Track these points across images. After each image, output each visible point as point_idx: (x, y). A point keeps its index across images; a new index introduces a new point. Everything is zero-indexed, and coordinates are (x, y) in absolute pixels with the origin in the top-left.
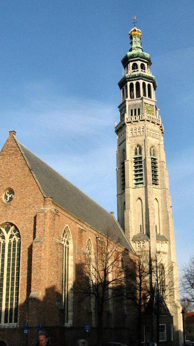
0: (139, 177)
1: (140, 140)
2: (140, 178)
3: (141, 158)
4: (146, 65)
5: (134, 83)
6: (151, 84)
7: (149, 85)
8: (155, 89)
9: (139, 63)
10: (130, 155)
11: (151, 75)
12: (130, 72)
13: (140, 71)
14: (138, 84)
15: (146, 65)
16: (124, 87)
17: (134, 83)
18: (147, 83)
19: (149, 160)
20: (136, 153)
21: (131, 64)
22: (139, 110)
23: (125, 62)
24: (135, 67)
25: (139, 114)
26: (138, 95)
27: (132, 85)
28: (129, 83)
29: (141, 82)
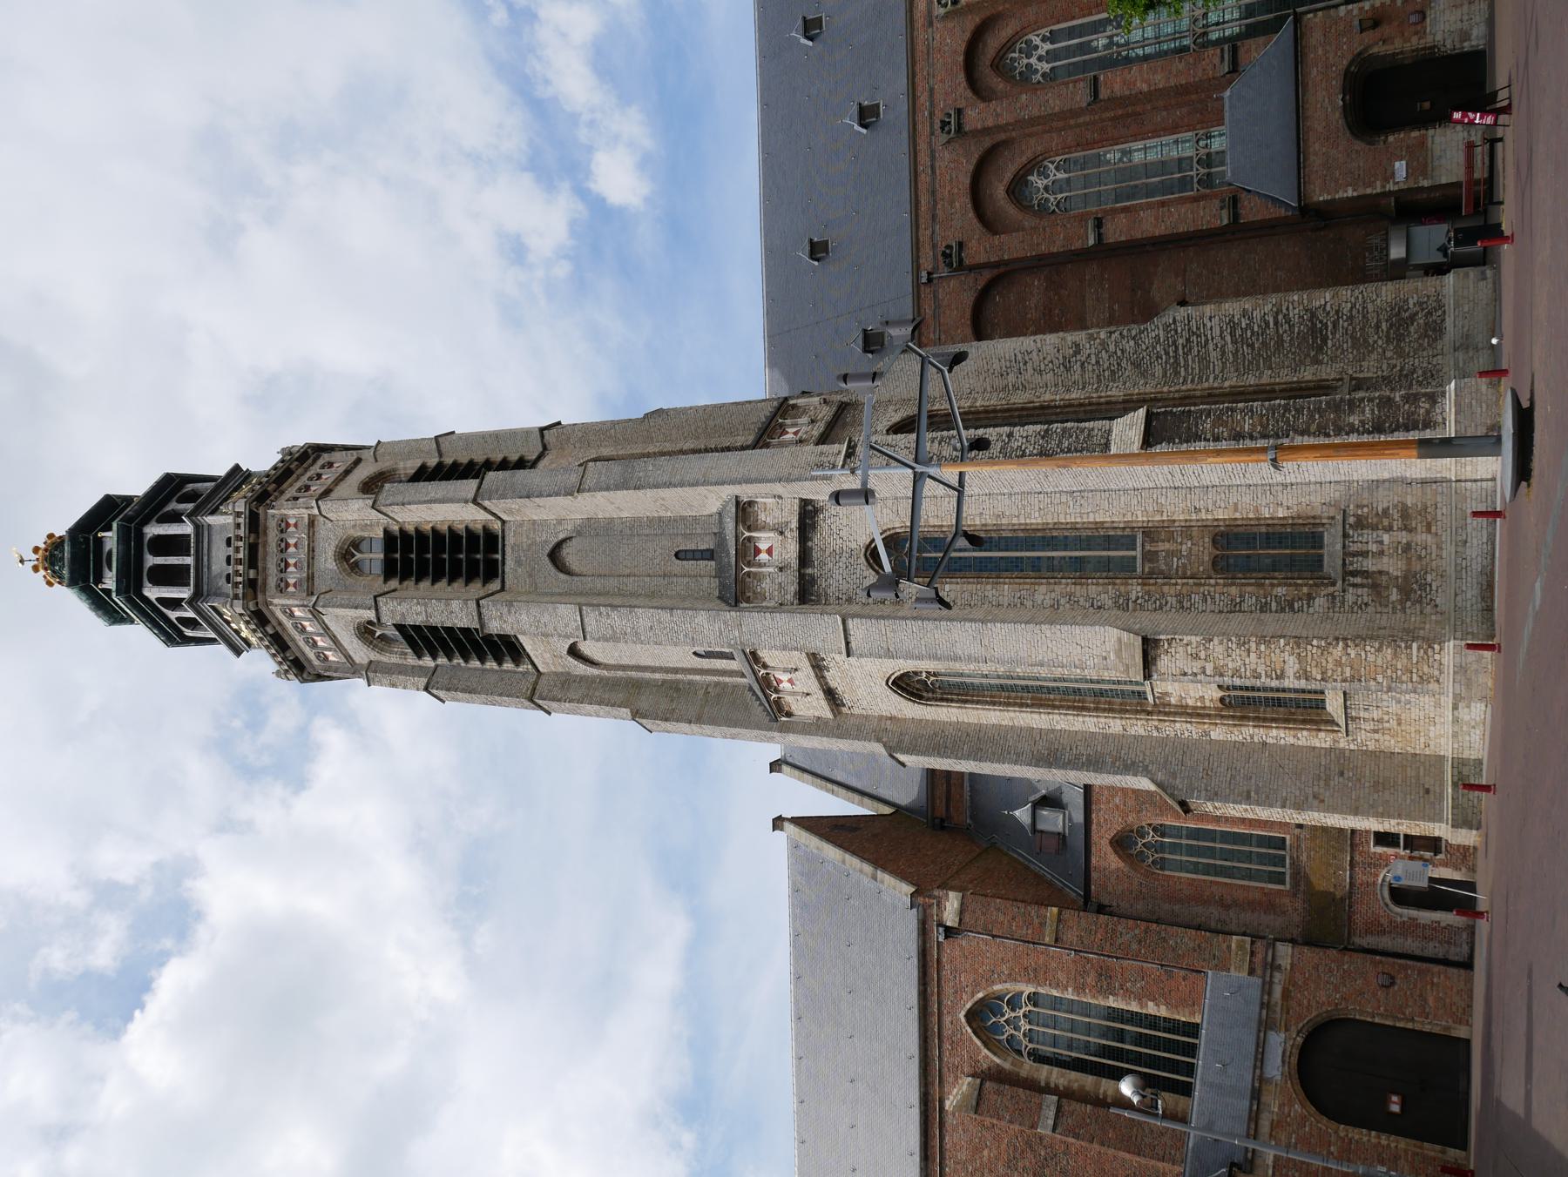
3: (389, 537)
5: (151, 560)
6: (190, 487)
16: (173, 615)
17: (151, 560)
18: (173, 506)
28: (152, 593)
29: (153, 530)
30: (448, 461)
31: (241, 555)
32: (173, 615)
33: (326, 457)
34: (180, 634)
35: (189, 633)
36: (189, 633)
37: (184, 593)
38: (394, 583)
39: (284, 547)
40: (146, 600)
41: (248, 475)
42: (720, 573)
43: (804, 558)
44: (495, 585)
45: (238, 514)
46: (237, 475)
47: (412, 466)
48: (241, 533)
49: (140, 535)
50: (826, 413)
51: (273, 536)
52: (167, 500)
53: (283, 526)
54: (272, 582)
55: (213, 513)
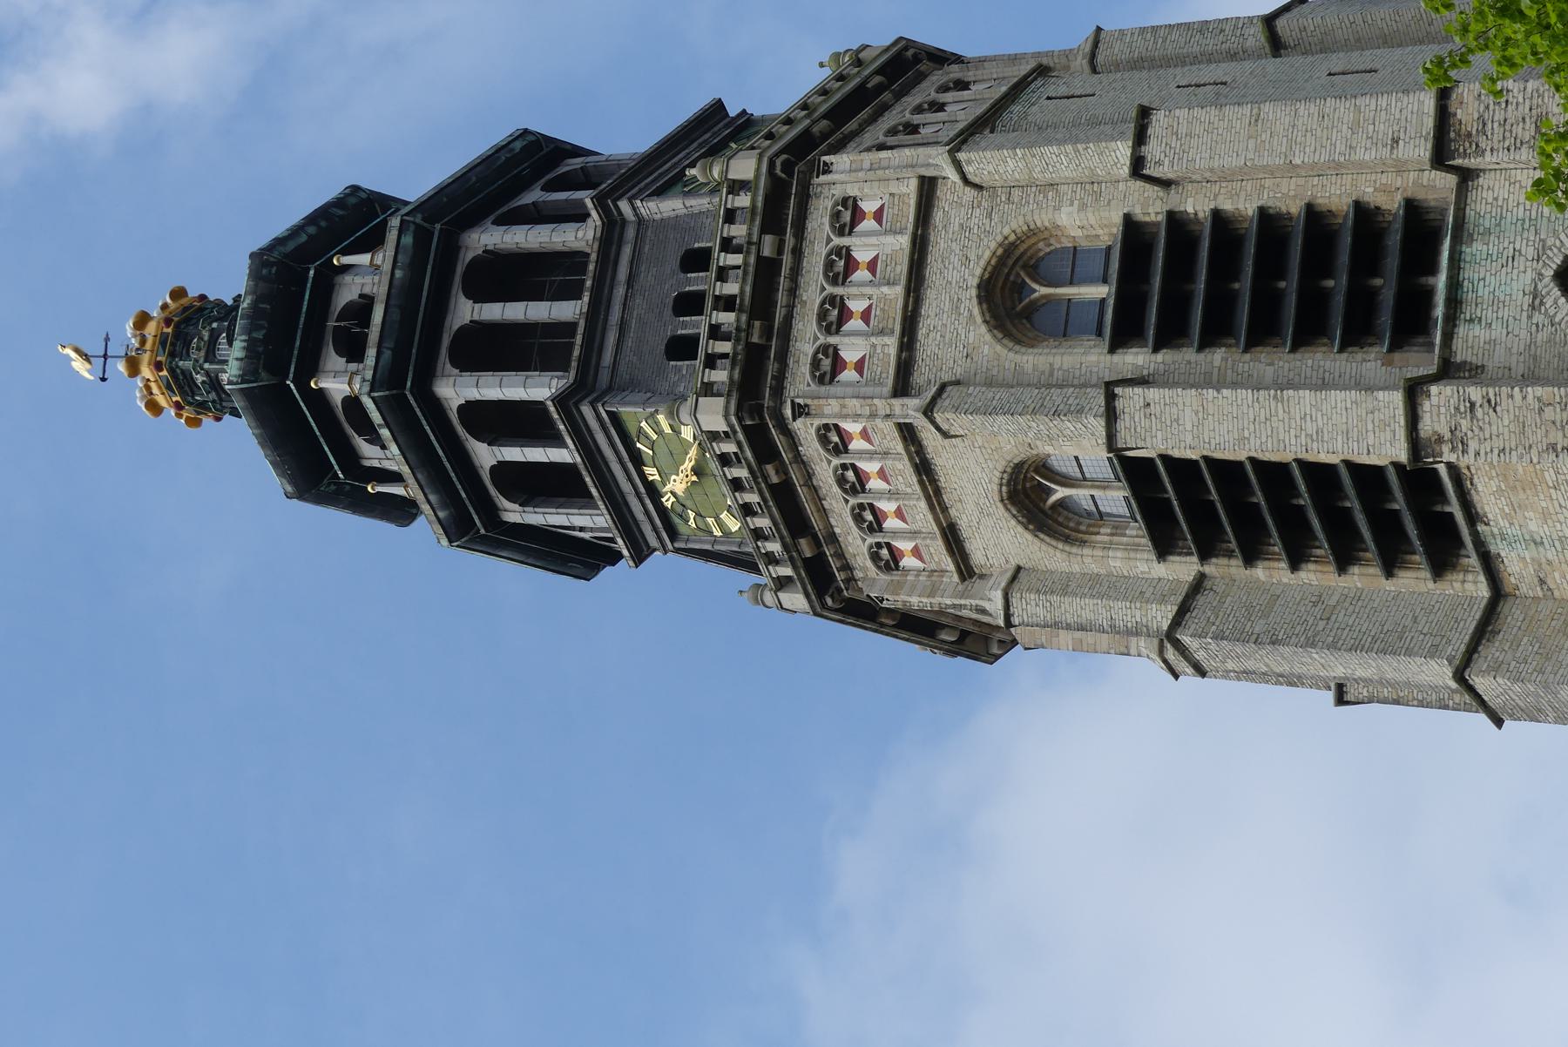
5: (465, 311)
17: (465, 311)
18: (534, 195)
31: (731, 288)
32: (486, 455)
34: (491, 512)
35: (513, 513)
36: (513, 513)
37: (539, 388)
38: (1135, 359)
40: (435, 407)
41: (745, 126)
45: (736, 187)
46: (714, 130)
48: (738, 231)
49: (451, 248)
52: (524, 185)
53: (848, 215)
55: (660, 192)
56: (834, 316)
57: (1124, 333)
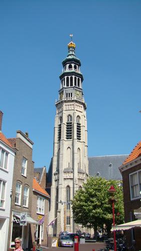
0: (69, 130)
1: (71, 113)
2: (69, 136)
3: (71, 123)
4: (77, 66)
5: (69, 77)
6: (80, 79)
7: (79, 79)
8: (82, 82)
9: (73, 65)
10: (65, 121)
11: (80, 73)
12: (67, 70)
13: (73, 70)
14: (71, 78)
15: (77, 66)
17: (69, 77)
18: (77, 78)
19: (75, 126)
20: (68, 120)
21: (68, 65)
22: (71, 93)
23: (64, 64)
24: (70, 67)
25: (72, 96)
26: (72, 85)
27: (68, 78)
28: (66, 77)
29: (74, 77)
30: (81, 128)
33: (82, 106)
39: (71, 105)
42: (67, 169)
43: (68, 179)
44: (66, 140)
47: (81, 122)
50: (83, 178)
51: (72, 103)
54: (66, 104)
56: (68, 105)
57: (67, 123)
